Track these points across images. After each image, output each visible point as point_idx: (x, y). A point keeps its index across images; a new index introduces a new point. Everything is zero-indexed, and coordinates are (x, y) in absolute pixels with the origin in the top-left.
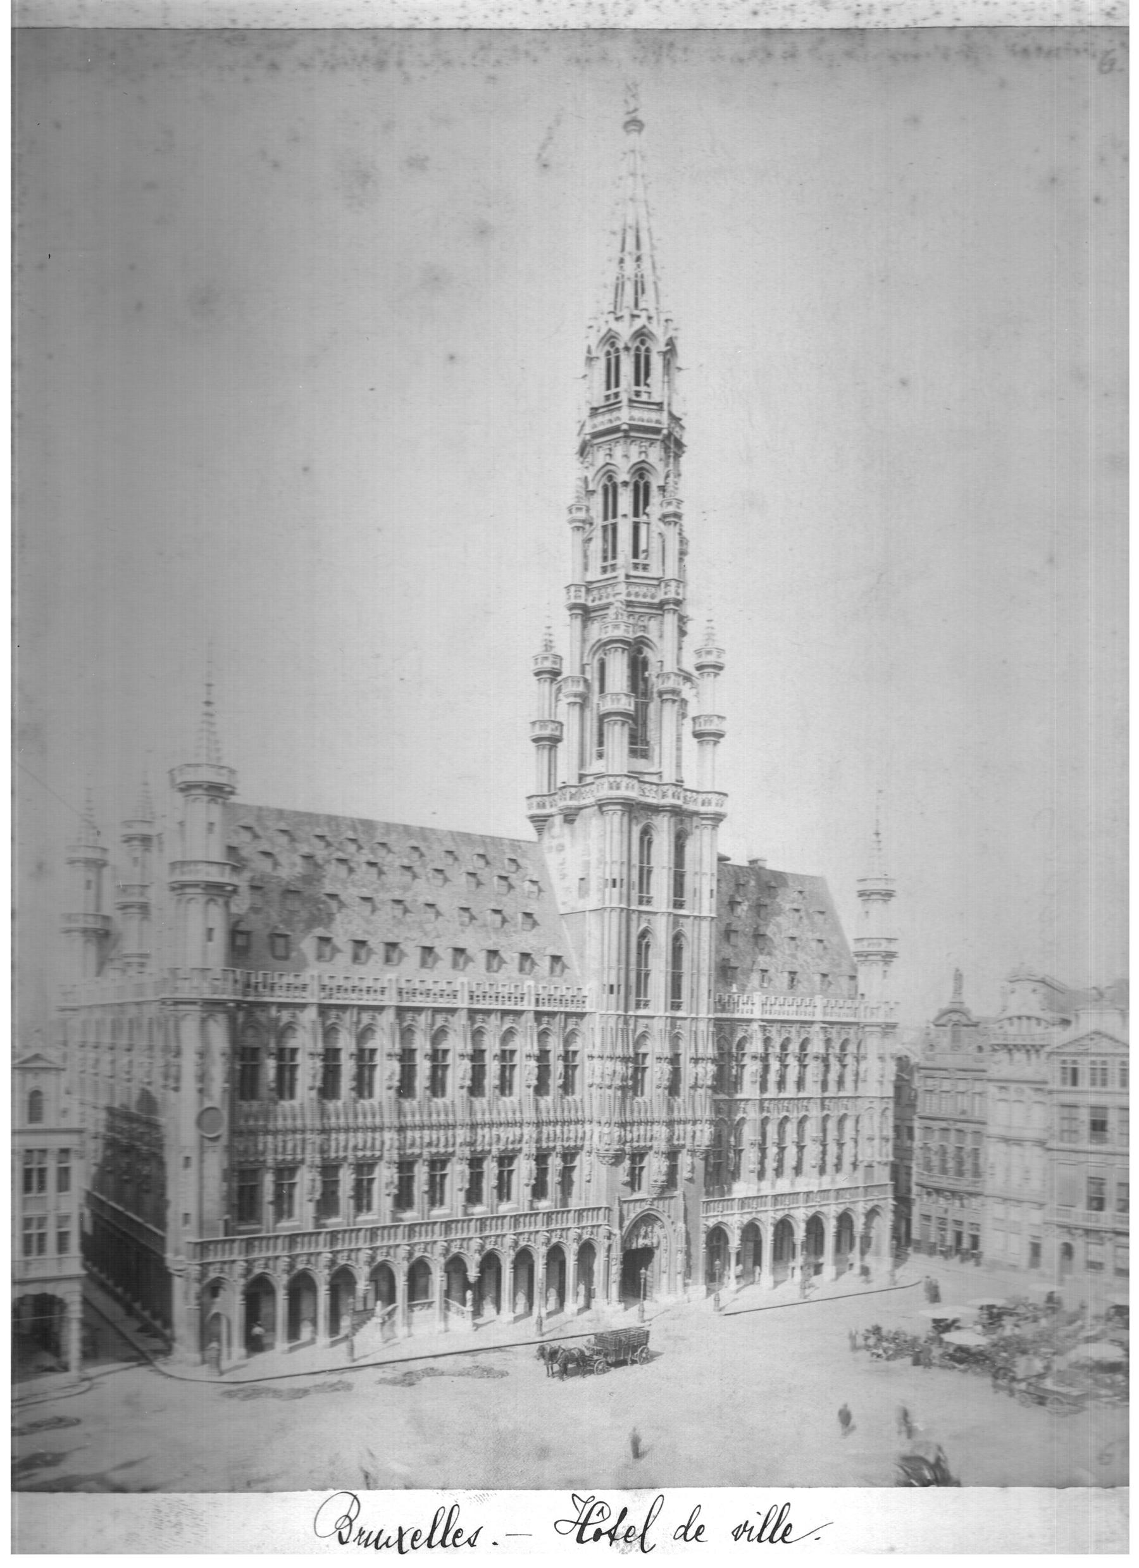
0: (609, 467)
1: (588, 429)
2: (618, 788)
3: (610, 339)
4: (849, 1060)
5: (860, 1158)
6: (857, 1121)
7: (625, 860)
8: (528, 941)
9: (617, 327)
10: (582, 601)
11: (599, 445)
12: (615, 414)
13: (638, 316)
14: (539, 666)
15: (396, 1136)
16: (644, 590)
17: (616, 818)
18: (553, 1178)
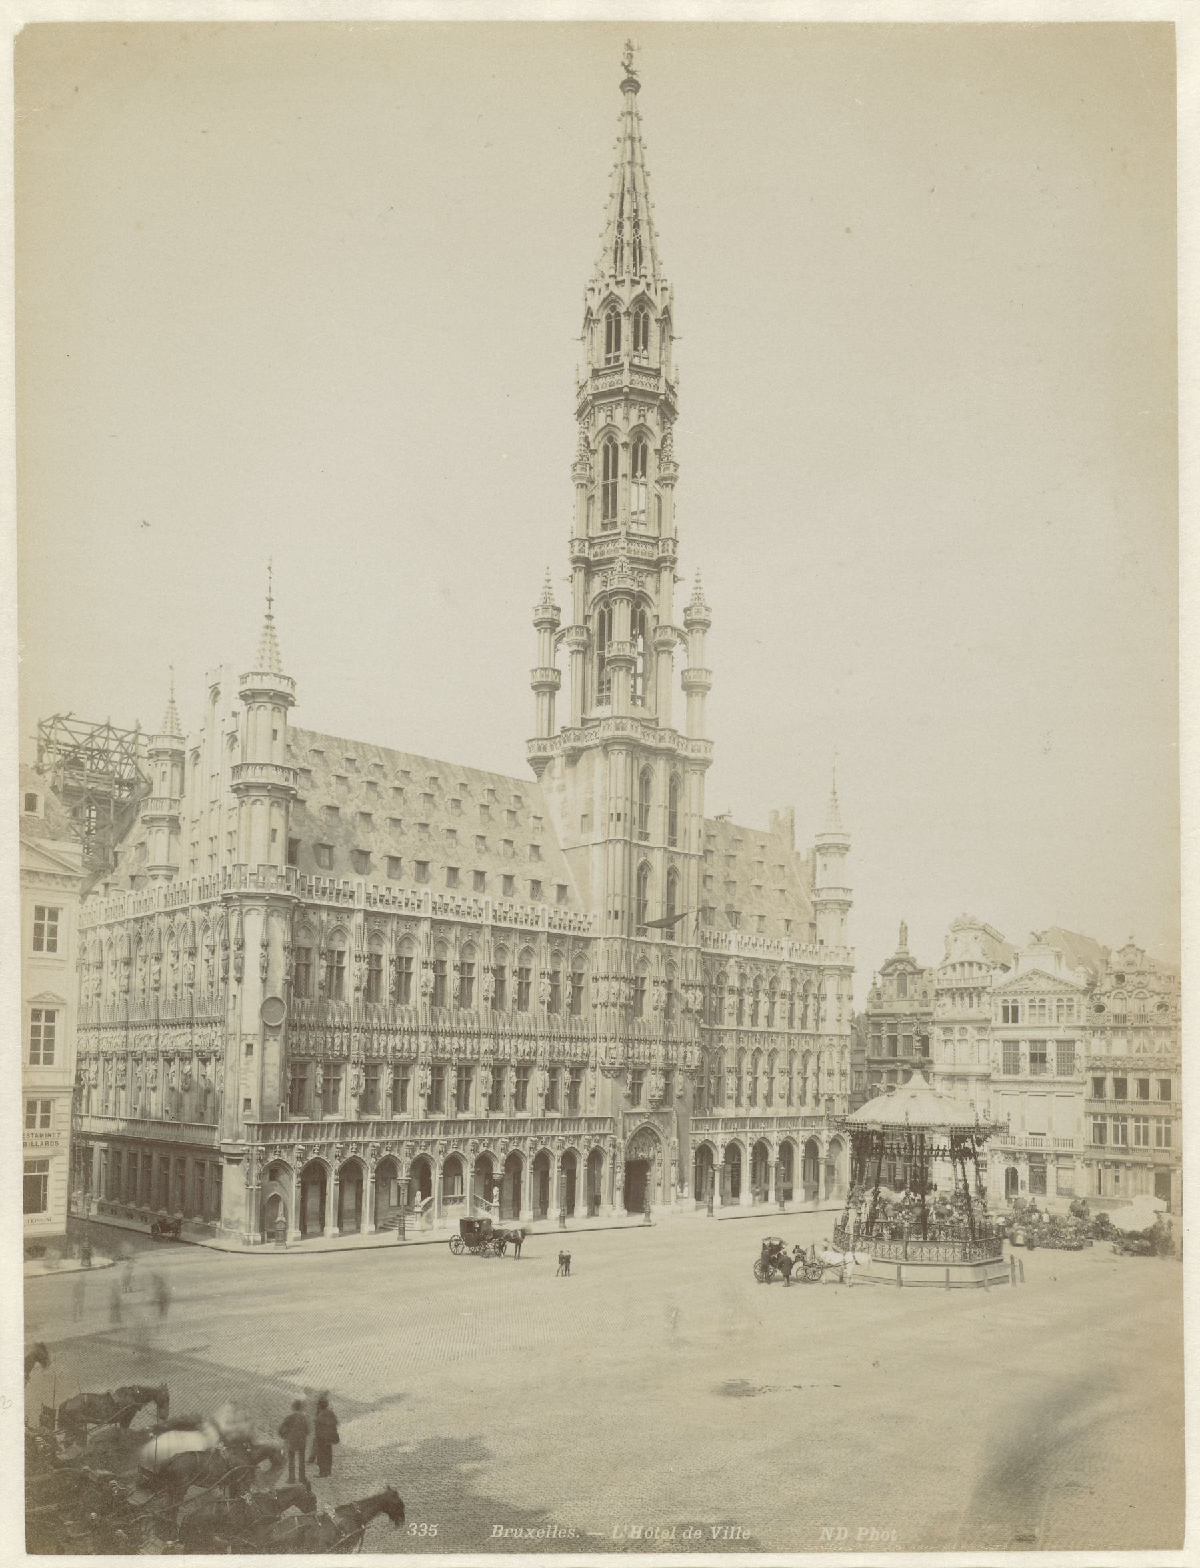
0: (610, 428)
1: (590, 390)
2: (623, 729)
3: (611, 302)
4: (811, 1000)
5: (821, 1092)
6: (818, 1059)
7: (628, 795)
8: (537, 871)
9: (617, 291)
10: (586, 555)
11: (601, 407)
12: (617, 377)
13: (638, 283)
14: (541, 616)
15: (430, 1039)
16: (642, 548)
17: (622, 757)
18: (563, 1090)
